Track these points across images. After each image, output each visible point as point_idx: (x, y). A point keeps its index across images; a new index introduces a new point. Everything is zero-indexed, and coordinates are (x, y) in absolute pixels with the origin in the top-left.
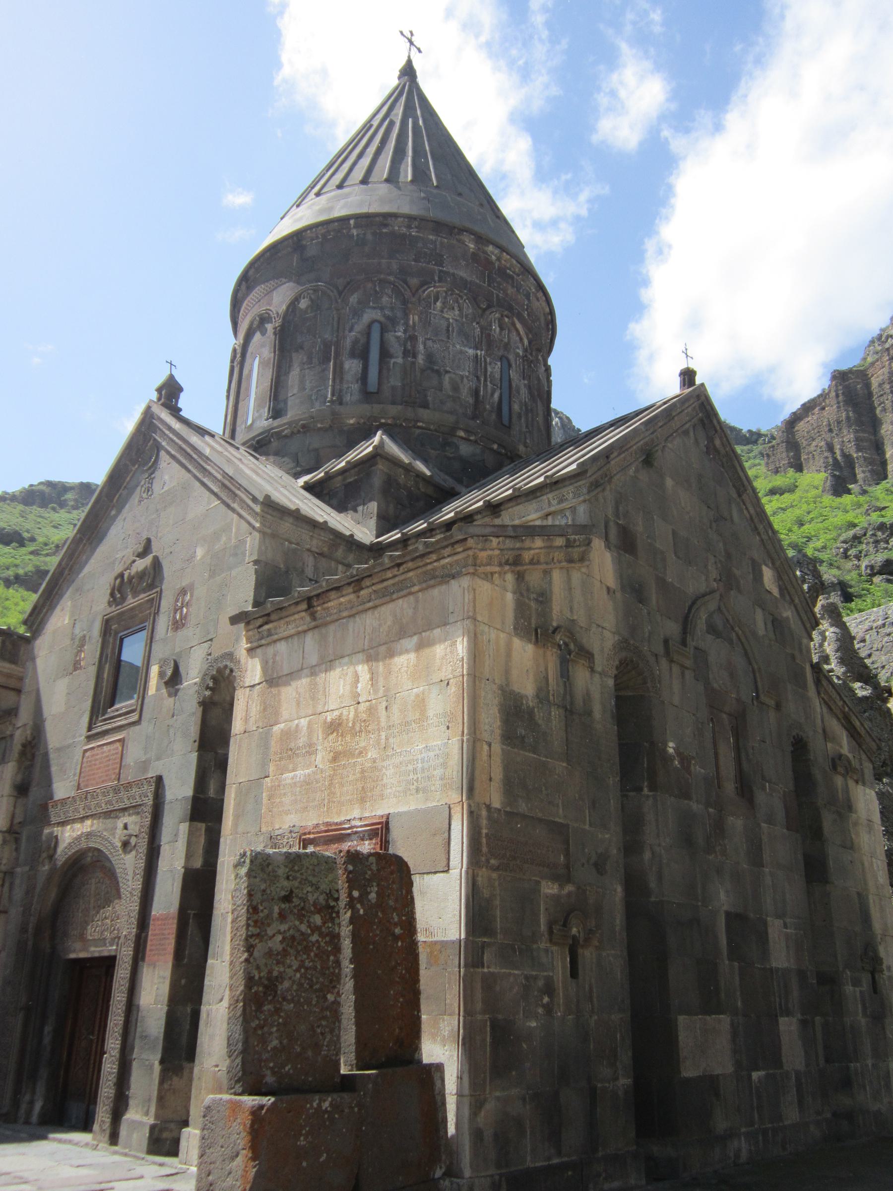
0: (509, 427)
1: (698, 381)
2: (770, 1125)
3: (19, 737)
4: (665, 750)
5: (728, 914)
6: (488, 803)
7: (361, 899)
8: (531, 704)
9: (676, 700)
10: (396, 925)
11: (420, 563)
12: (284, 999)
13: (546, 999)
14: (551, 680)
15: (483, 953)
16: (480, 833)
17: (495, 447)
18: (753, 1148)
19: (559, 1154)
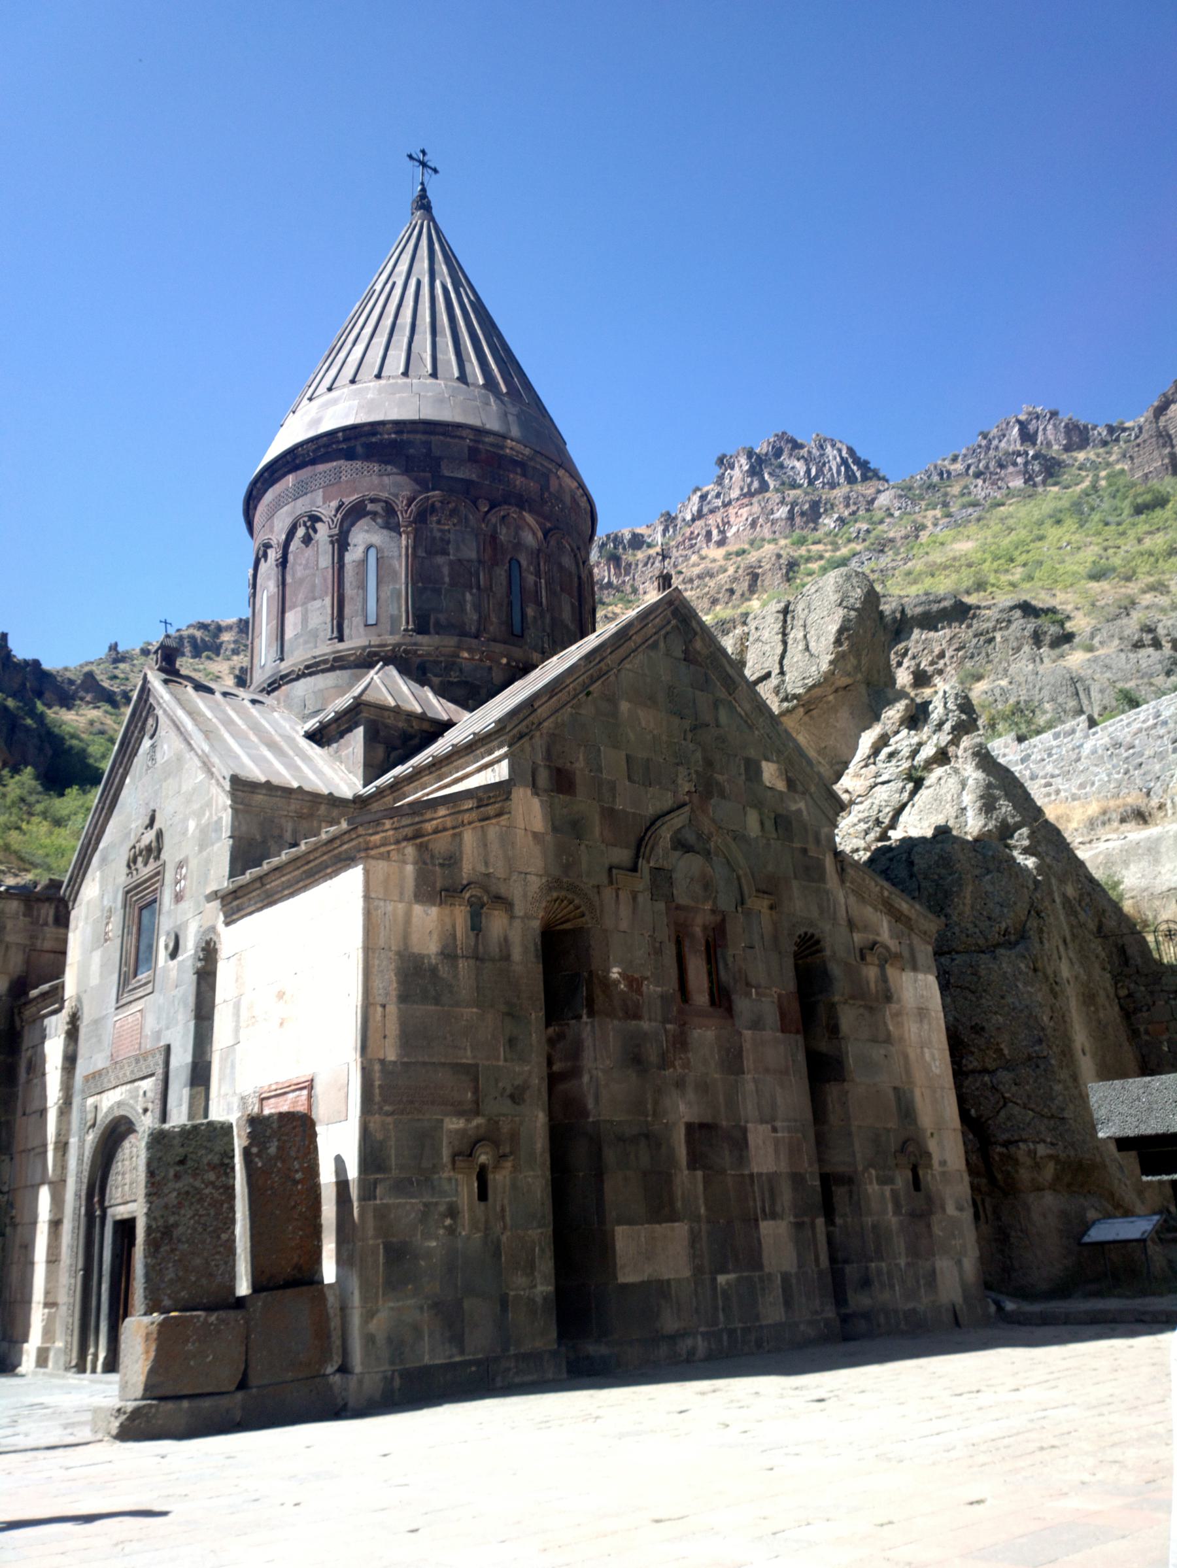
0: (522, 636)
2: (741, 1325)
4: (607, 977)
5: (689, 1127)
6: (382, 1057)
7: (259, 1155)
8: (434, 961)
9: (624, 925)
10: (297, 1171)
12: (179, 1241)
13: (448, 1222)
14: (459, 934)
15: (375, 1188)
16: (372, 1085)
18: (713, 1347)
19: (462, 1352)
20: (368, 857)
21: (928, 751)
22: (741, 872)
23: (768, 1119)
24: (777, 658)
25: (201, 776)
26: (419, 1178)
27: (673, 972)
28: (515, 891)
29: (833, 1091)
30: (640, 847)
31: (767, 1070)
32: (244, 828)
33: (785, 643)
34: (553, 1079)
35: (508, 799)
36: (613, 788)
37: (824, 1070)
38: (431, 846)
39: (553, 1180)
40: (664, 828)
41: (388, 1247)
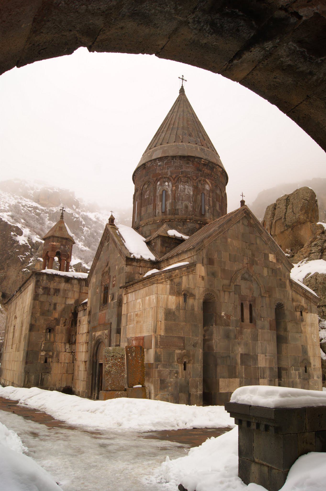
0: (204, 215)
1: (245, 204)
3: (88, 309)
5: (241, 354)
13: (176, 375)
14: (181, 303)
16: (157, 341)
17: (199, 222)
20: (157, 283)
23: (264, 353)
24: (284, 214)
26: (169, 364)
29: (284, 346)
30: (232, 280)
31: (265, 340)
32: (129, 270)
33: (286, 209)
34: (205, 341)
37: (280, 340)
38: (174, 280)
39: (204, 366)
41: (160, 380)
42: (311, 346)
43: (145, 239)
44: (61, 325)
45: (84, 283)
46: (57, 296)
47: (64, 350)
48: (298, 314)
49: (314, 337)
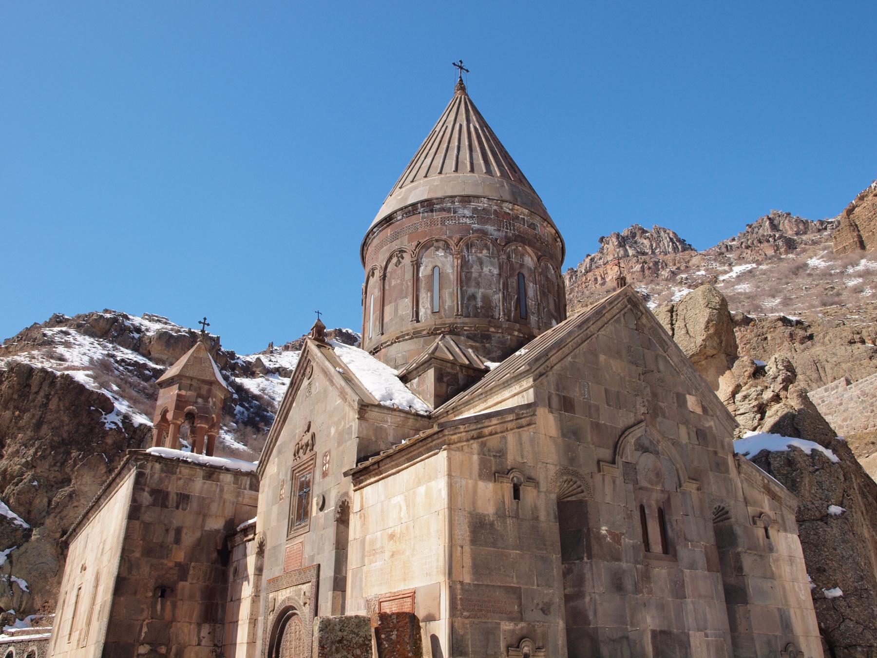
5: (654, 633)
9: (608, 499)
10: (409, 652)
11: (424, 443)
14: (506, 502)
21: (768, 395)
22: (678, 466)
25: (339, 401)
27: (639, 530)
28: (541, 477)
29: (740, 609)
30: (616, 448)
31: (700, 596)
32: (365, 432)
34: (568, 598)
35: (534, 415)
36: (598, 410)
38: (488, 444)
40: (630, 436)
42: (798, 611)
43: (396, 372)
44: (189, 579)
45: (247, 481)
46: (184, 509)
47: (195, 641)
48: (761, 532)
49: (799, 587)
